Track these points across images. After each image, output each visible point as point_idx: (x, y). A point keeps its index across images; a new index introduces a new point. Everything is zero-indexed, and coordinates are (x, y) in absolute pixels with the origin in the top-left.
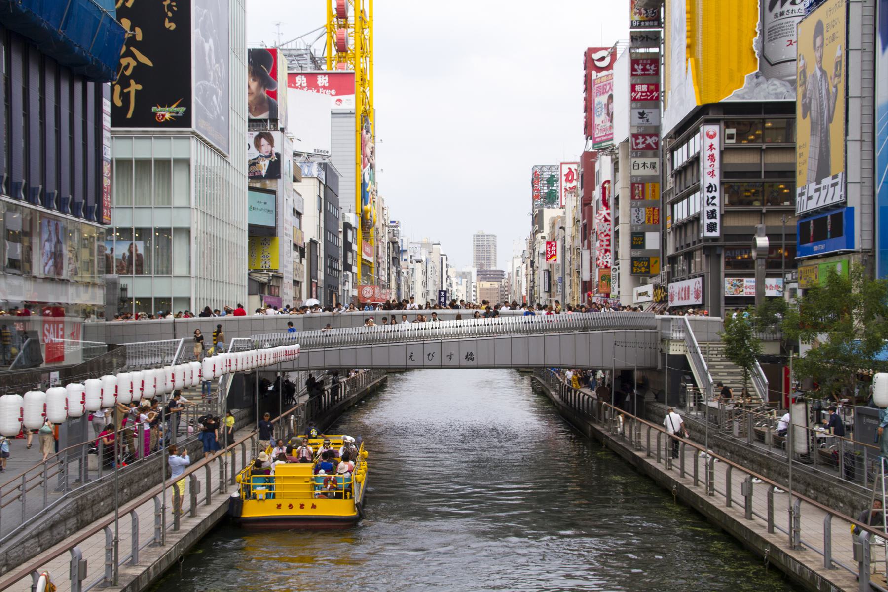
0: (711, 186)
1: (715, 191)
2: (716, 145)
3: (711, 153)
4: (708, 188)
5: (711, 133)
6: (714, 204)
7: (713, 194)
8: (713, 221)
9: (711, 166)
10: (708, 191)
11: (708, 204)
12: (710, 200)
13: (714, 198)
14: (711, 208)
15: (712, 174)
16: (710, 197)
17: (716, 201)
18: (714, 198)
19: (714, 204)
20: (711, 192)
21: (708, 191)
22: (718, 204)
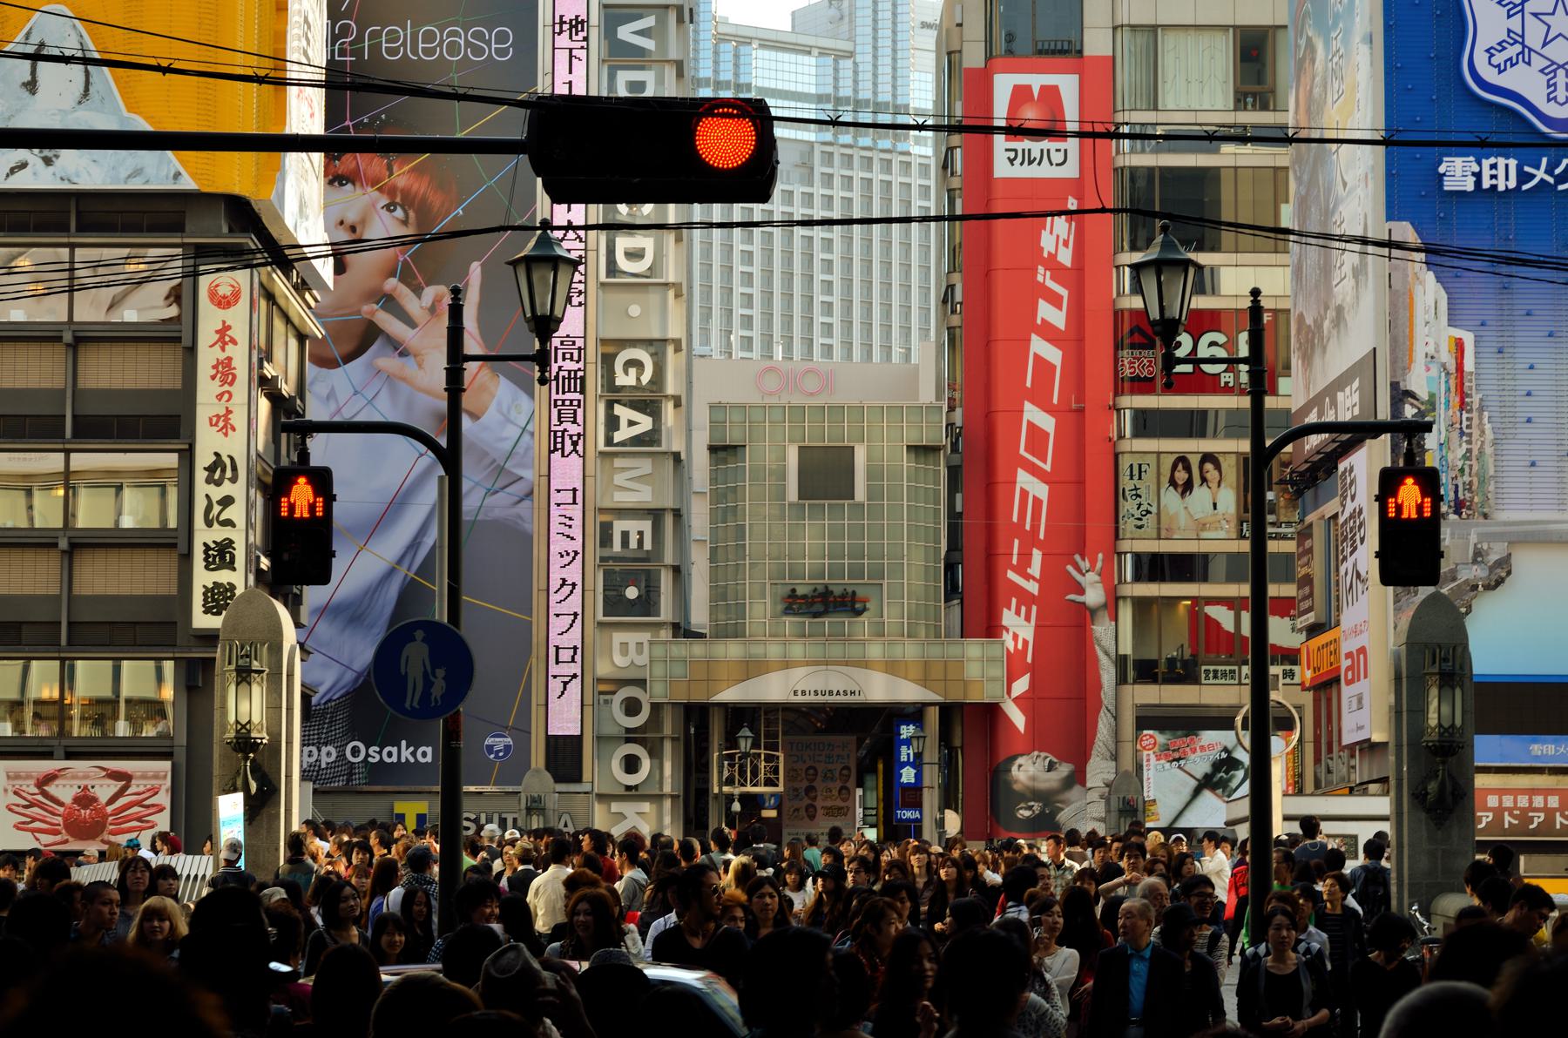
0: (218, 464)
1: (234, 480)
2: (240, 332)
3: (222, 356)
4: (211, 469)
5: (224, 290)
6: (229, 523)
7: (227, 489)
8: (224, 576)
9: (220, 397)
10: (208, 481)
11: (209, 523)
12: (216, 509)
13: (227, 501)
14: (218, 534)
15: (223, 423)
16: (216, 497)
17: (236, 513)
18: (227, 501)
19: (229, 523)
20: (218, 483)
21: (208, 481)
22: (241, 522)
